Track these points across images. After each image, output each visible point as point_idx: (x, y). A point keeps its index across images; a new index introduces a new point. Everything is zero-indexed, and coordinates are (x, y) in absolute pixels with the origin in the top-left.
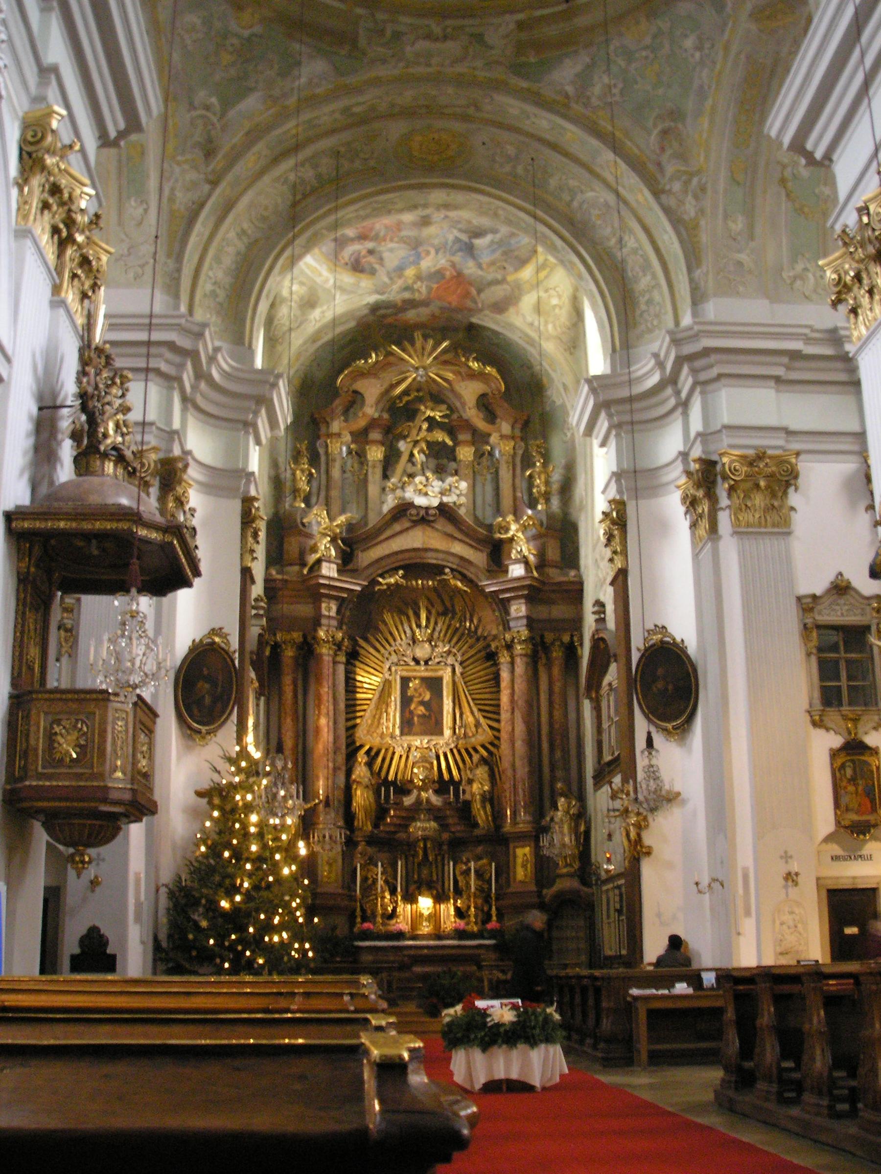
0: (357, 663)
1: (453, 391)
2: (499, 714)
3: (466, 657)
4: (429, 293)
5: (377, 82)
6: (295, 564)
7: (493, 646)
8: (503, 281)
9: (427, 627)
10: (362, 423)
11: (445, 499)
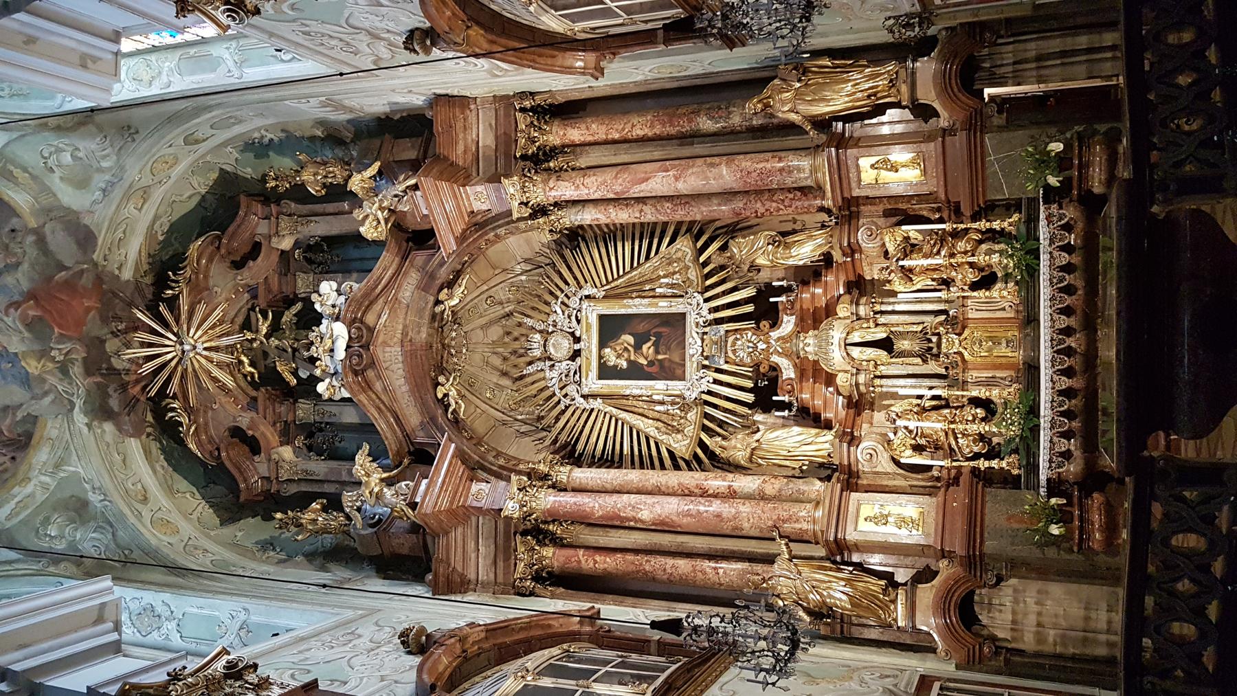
4: (70, 339)
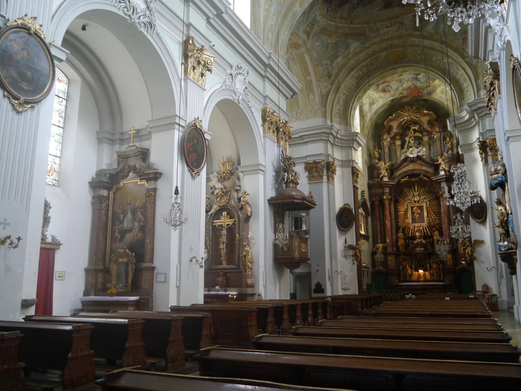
0: (398, 204)
1: (420, 120)
2: (441, 215)
3: (430, 199)
5: (374, 44)
6: (376, 178)
7: (438, 195)
8: (429, 86)
9: (418, 191)
10: (392, 134)
11: (419, 154)
